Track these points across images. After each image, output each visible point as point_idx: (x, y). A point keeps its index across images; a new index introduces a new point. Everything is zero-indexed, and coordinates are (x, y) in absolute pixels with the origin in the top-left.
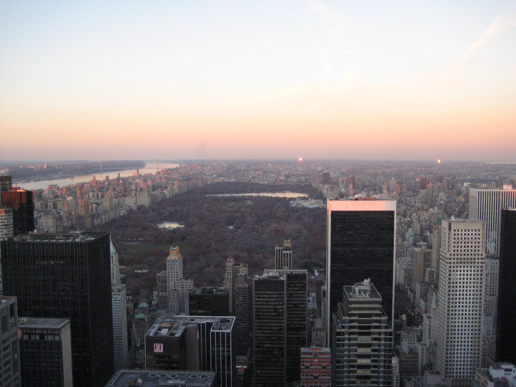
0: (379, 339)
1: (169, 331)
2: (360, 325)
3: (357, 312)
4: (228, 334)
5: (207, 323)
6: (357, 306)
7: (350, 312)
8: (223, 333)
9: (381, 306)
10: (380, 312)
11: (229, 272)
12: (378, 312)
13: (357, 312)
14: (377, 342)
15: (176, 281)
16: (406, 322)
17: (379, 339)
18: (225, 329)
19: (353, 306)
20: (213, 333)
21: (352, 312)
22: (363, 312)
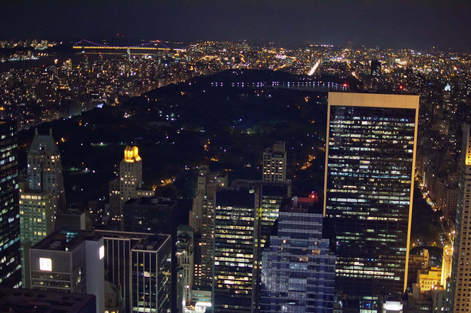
0: (318, 268)
1: (62, 244)
2: (293, 248)
3: (289, 230)
4: (153, 255)
5: (132, 241)
6: (290, 222)
7: (279, 230)
8: (147, 254)
9: (321, 225)
10: (320, 233)
11: (201, 182)
12: (316, 232)
13: (289, 230)
14: (315, 271)
15: (131, 192)
16: (427, 259)
17: (318, 268)
18: (150, 250)
19: (283, 222)
20: (134, 254)
21: (283, 230)
22: (297, 231)
